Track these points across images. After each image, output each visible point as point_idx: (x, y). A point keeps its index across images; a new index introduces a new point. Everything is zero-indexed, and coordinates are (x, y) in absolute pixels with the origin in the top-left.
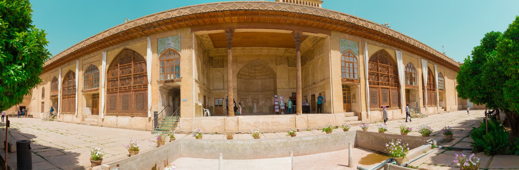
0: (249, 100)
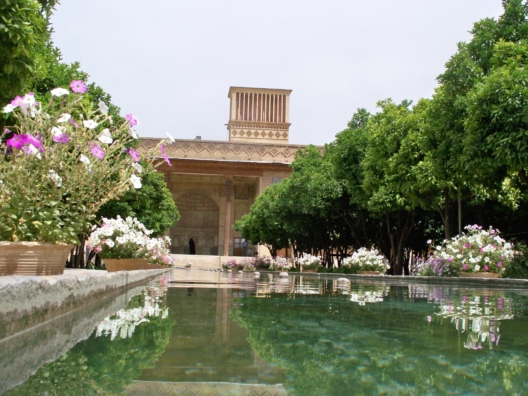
0: (185, 238)
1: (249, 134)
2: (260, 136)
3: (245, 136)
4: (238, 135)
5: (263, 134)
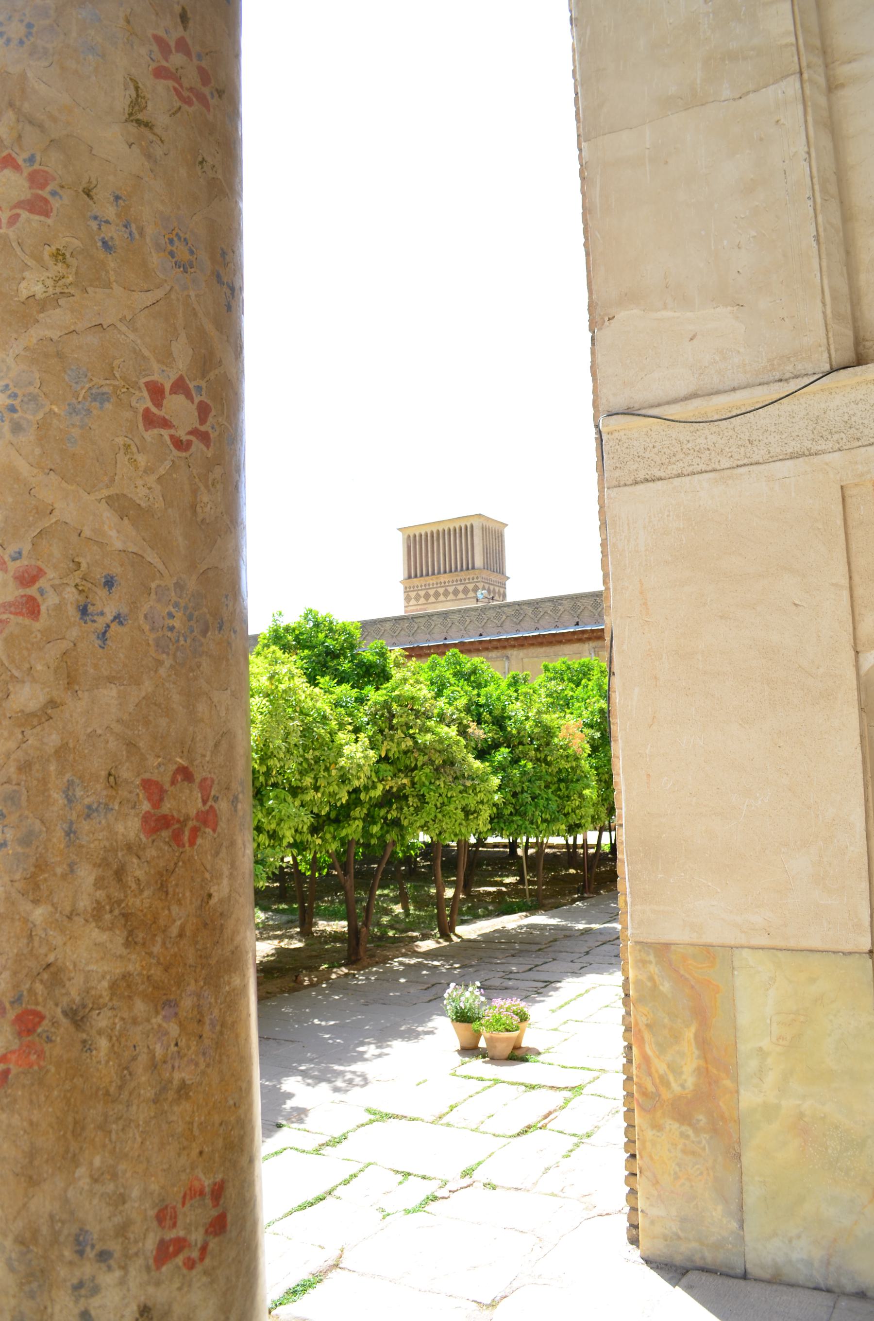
1: (427, 596)
2: (442, 598)
3: (422, 601)
4: (413, 602)
5: (446, 593)
